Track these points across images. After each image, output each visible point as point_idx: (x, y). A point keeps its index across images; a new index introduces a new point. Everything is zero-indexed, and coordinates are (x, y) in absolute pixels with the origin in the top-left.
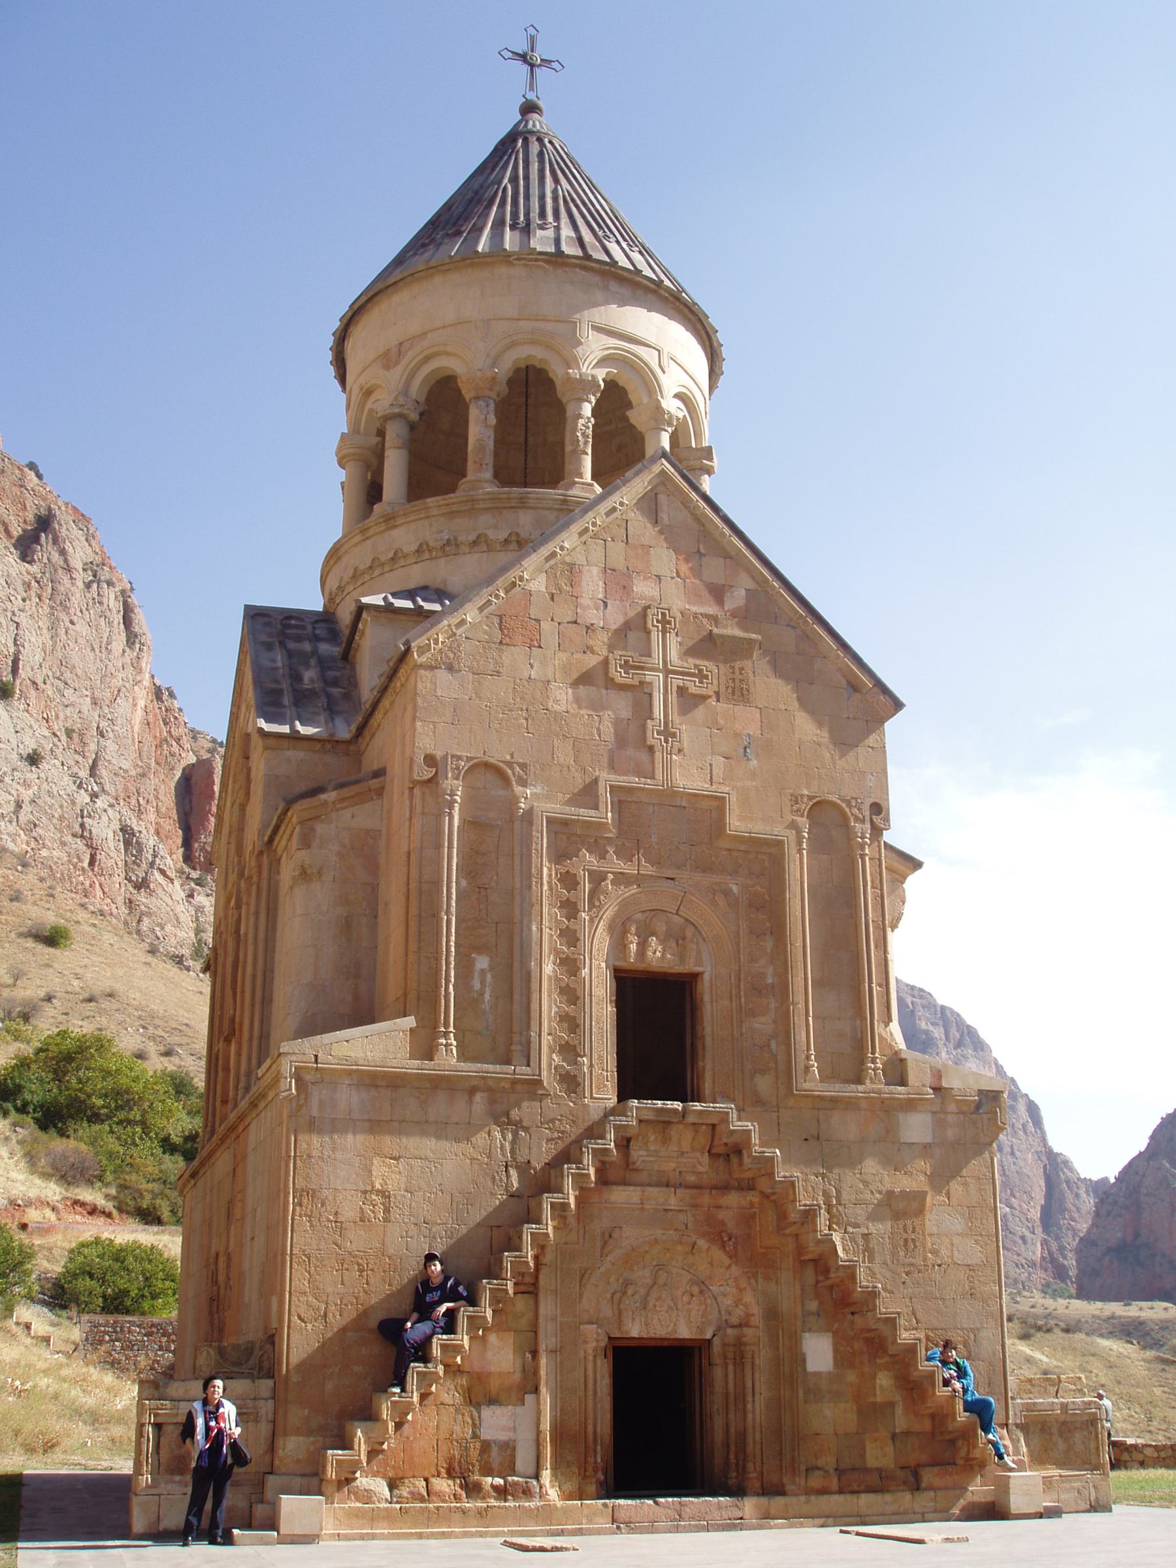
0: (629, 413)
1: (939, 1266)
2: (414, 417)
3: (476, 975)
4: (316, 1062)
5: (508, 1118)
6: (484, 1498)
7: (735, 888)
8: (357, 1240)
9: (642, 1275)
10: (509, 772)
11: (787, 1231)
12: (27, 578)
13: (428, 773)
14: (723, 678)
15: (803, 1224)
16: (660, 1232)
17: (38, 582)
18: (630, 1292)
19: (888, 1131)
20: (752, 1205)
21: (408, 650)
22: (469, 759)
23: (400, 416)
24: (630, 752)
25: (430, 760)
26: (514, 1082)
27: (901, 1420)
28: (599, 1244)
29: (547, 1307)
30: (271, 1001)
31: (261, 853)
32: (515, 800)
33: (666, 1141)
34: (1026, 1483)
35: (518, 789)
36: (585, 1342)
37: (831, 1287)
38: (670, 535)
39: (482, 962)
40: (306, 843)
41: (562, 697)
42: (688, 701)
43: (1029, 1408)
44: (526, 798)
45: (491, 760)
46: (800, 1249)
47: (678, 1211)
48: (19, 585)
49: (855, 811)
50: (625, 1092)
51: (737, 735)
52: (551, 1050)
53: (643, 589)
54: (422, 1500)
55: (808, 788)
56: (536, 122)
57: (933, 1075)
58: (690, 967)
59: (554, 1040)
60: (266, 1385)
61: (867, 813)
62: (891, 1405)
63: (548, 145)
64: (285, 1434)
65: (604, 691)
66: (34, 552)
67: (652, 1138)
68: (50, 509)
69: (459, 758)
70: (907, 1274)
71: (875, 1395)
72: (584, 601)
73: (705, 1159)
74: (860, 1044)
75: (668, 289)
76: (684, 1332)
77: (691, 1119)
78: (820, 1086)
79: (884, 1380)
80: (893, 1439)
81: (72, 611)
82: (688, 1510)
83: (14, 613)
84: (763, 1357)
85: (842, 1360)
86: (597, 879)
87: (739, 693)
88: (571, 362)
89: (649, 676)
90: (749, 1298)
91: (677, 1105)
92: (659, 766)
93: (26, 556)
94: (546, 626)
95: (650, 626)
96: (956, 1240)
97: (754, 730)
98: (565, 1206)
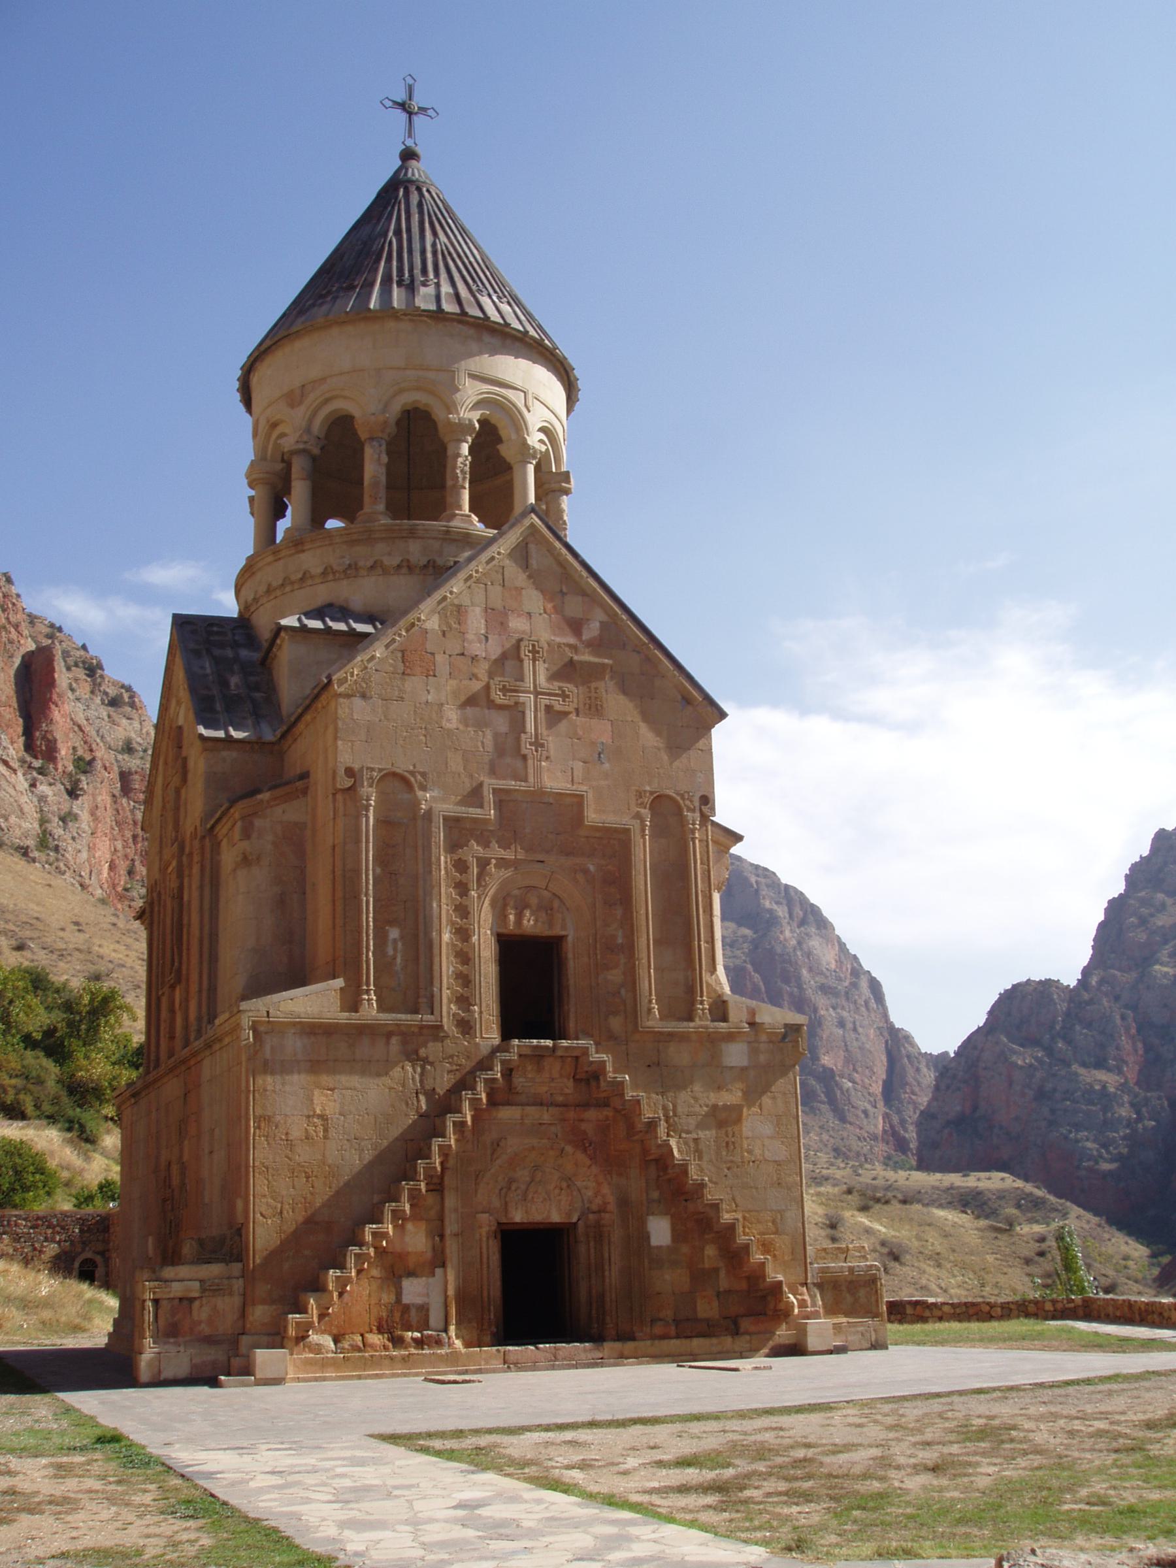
0: (499, 447)
2: (316, 451)
3: (390, 944)
4: (268, 1016)
5: (417, 1055)
6: (406, 1348)
7: (592, 868)
8: (303, 1154)
9: (523, 1175)
10: (412, 779)
11: (636, 1138)
13: (348, 783)
14: (581, 696)
15: (647, 1132)
18: (513, 1188)
20: (607, 1118)
21: (330, 681)
22: (380, 770)
23: (304, 451)
24: (508, 760)
25: (350, 772)
26: (422, 1027)
27: (724, 1282)
28: (489, 1152)
29: (450, 1201)
30: (217, 961)
31: (203, 837)
32: (416, 803)
33: (540, 1070)
34: (820, 1329)
35: (420, 794)
36: (480, 1227)
37: (669, 1180)
38: (535, 578)
39: (394, 933)
40: (246, 835)
41: (452, 717)
42: (554, 716)
43: (823, 1270)
45: (398, 771)
46: (645, 1151)
49: (688, 802)
50: (508, 1032)
51: (593, 743)
52: (450, 1002)
53: (517, 624)
54: (359, 1350)
55: (650, 785)
56: (417, 170)
58: (557, 931)
60: (236, 1268)
61: (697, 804)
62: (716, 1270)
63: (426, 194)
64: (254, 1304)
65: (487, 711)
67: (529, 1068)
69: (372, 769)
70: (728, 1169)
72: (470, 636)
73: (571, 1083)
74: (691, 990)
75: (532, 338)
76: (556, 1218)
77: (559, 1053)
78: (660, 1024)
79: (710, 1251)
84: (617, 1235)
85: (677, 1236)
86: (483, 863)
87: (594, 708)
88: (451, 407)
89: (523, 697)
90: (606, 1190)
91: (549, 1043)
92: (531, 771)
94: (439, 658)
95: (522, 656)
96: (767, 1142)
97: (606, 738)
98: (463, 1124)
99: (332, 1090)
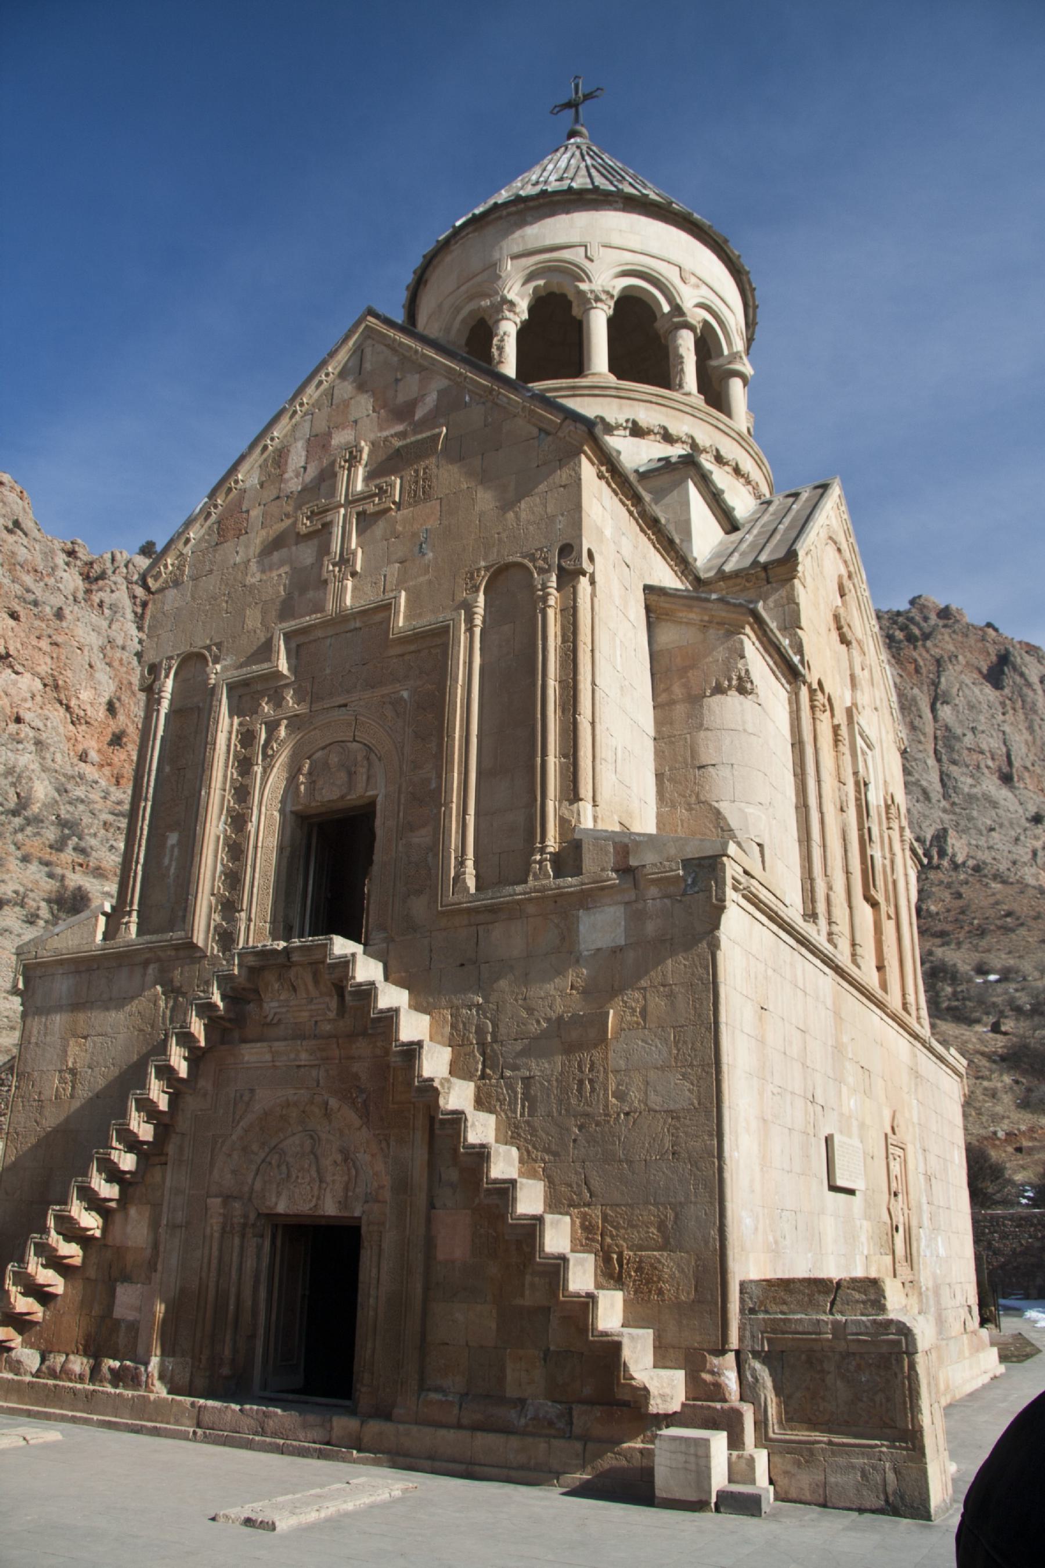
1: (627, 1114)
3: (168, 851)
6: (101, 1381)
7: (405, 694)
10: (207, 654)
12: (1001, 699)
16: (292, 1092)
17: (1010, 700)
19: (563, 939)
43: (774, 1327)
44: (216, 674)
45: (196, 650)
47: (312, 1066)
48: (997, 705)
49: (541, 563)
57: (616, 853)
58: (358, 794)
59: (217, 901)
65: (294, 548)
66: (1002, 681)
68: (1006, 650)
70: (581, 1128)
71: (522, 1295)
76: (330, 1208)
80: (545, 1360)
81: (1040, 712)
82: (271, 1423)
83: (999, 725)
93: (998, 685)
96: (652, 1075)
99: (85, 1038)
